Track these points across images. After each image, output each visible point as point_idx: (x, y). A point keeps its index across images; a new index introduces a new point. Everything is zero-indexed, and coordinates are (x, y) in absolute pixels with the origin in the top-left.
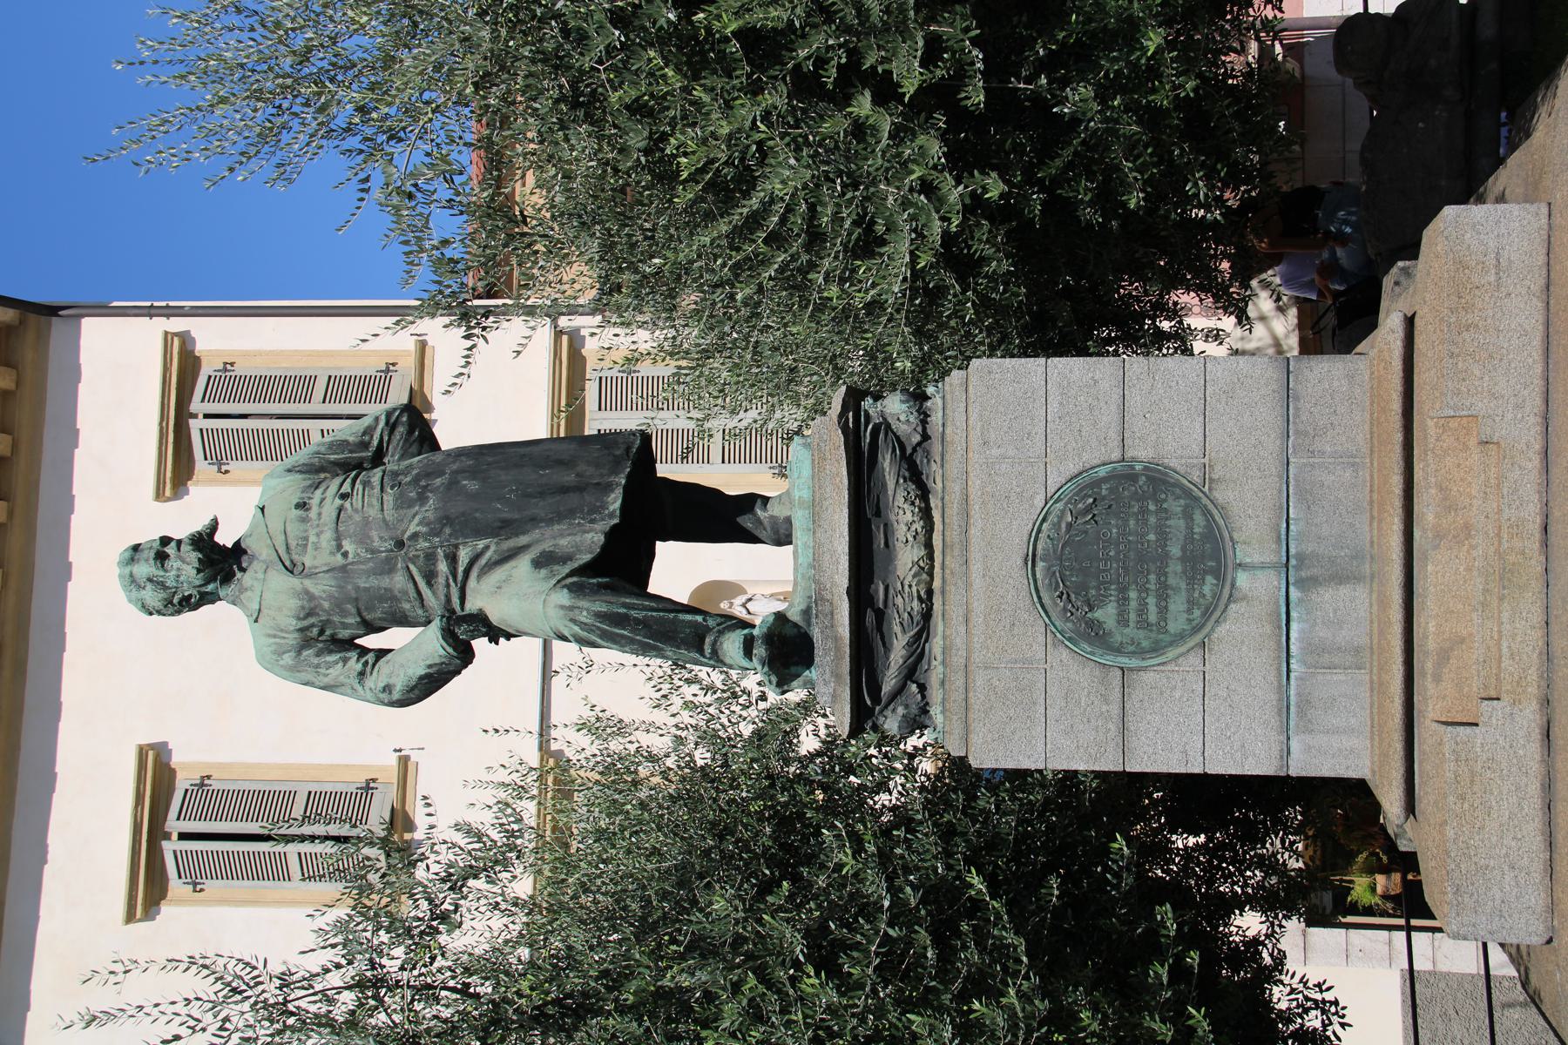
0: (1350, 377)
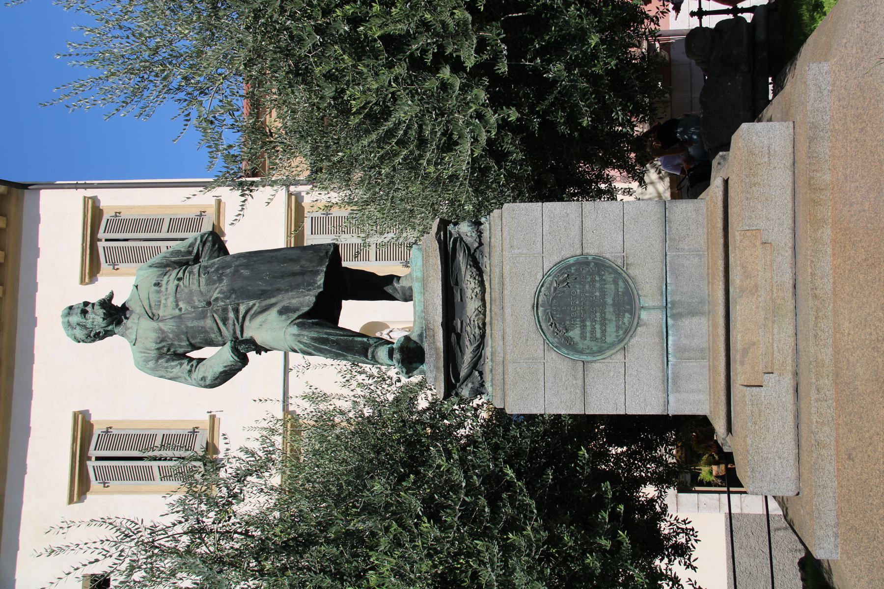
0: (697, 211)
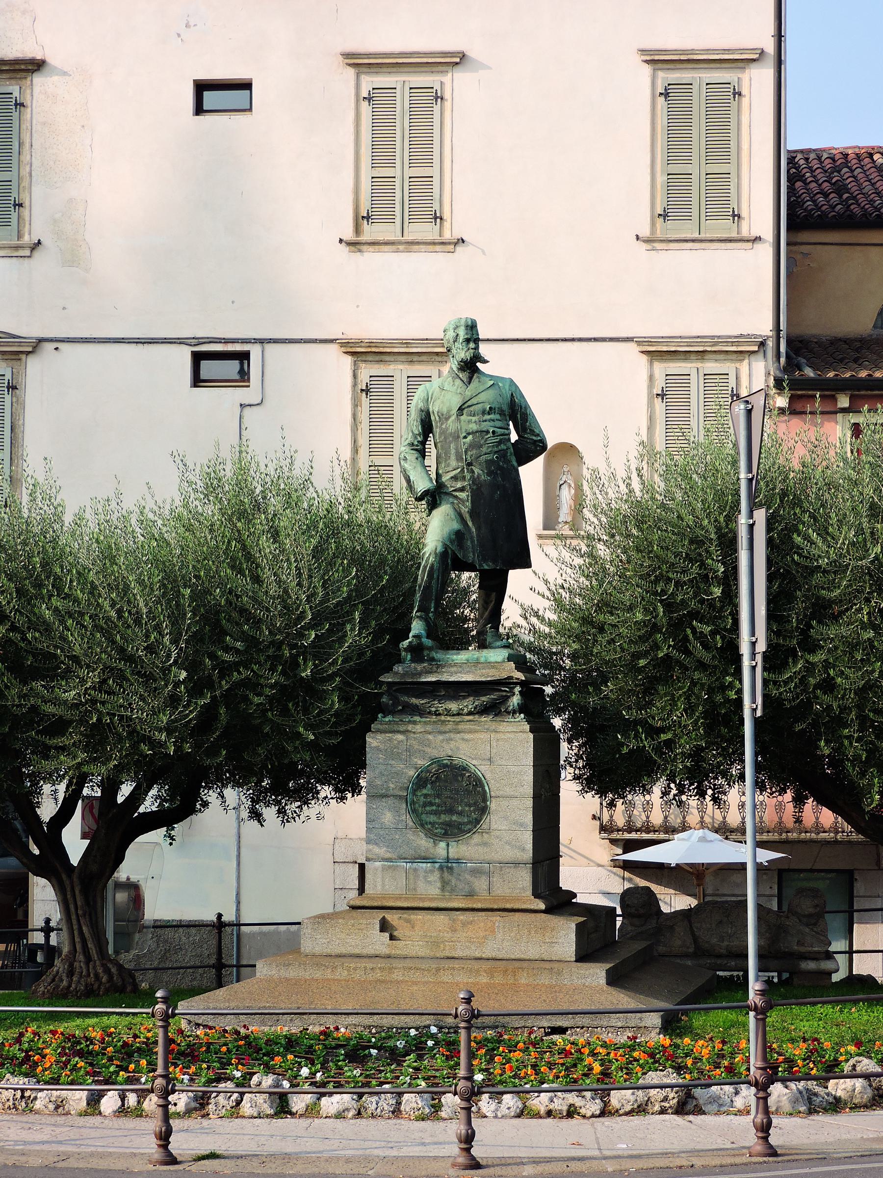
0: (523, 888)
